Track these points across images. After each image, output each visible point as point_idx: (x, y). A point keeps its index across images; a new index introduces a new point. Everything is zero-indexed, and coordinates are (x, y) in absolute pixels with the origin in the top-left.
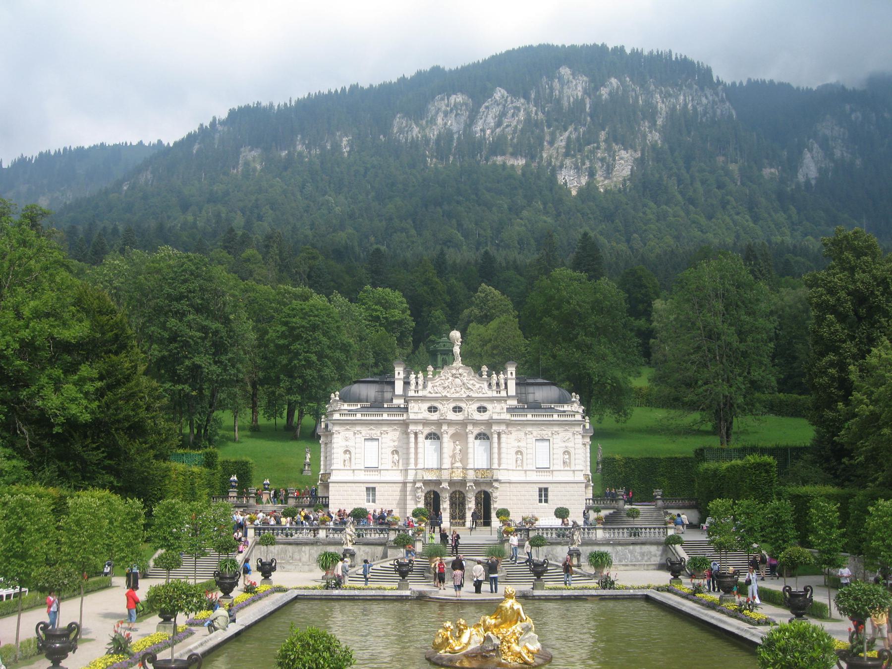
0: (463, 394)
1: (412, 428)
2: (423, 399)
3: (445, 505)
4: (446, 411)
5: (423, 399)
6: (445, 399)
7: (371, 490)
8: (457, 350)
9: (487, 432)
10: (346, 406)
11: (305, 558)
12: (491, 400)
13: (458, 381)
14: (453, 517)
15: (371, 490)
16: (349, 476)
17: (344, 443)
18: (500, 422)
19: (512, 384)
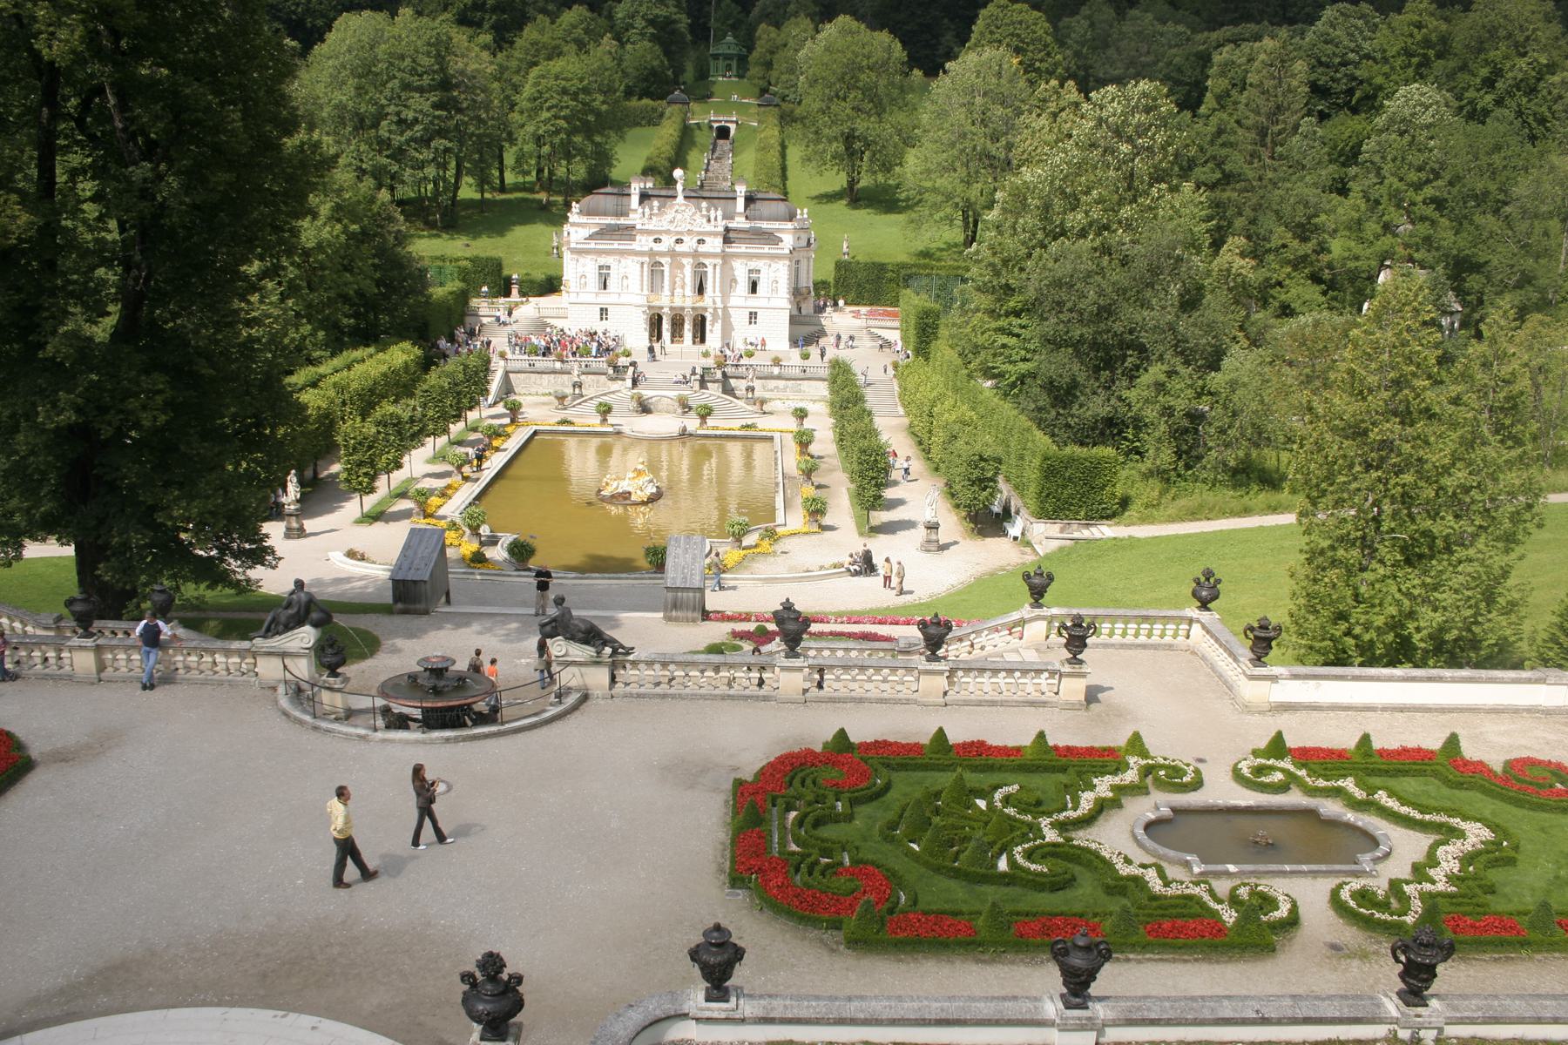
0: (684, 227)
1: (641, 259)
2: (649, 232)
3: (666, 326)
4: (668, 242)
5: (649, 232)
6: (667, 232)
7: (604, 312)
8: (679, 187)
9: (706, 261)
10: (584, 219)
11: (545, 383)
12: (710, 234)
13: (679, 216)
14: (673, 336)
15: (604, 312)
16: (583, 298)
17: (580, 269)
18: (714, 255)
19: (740, 203)
